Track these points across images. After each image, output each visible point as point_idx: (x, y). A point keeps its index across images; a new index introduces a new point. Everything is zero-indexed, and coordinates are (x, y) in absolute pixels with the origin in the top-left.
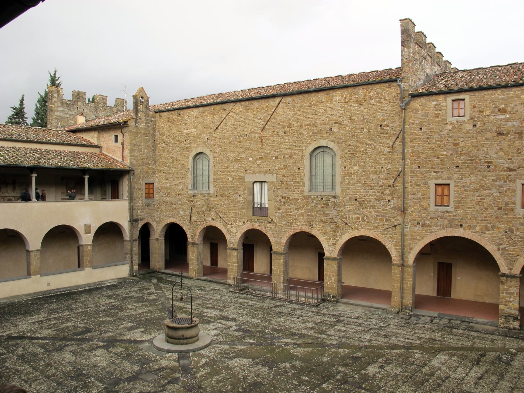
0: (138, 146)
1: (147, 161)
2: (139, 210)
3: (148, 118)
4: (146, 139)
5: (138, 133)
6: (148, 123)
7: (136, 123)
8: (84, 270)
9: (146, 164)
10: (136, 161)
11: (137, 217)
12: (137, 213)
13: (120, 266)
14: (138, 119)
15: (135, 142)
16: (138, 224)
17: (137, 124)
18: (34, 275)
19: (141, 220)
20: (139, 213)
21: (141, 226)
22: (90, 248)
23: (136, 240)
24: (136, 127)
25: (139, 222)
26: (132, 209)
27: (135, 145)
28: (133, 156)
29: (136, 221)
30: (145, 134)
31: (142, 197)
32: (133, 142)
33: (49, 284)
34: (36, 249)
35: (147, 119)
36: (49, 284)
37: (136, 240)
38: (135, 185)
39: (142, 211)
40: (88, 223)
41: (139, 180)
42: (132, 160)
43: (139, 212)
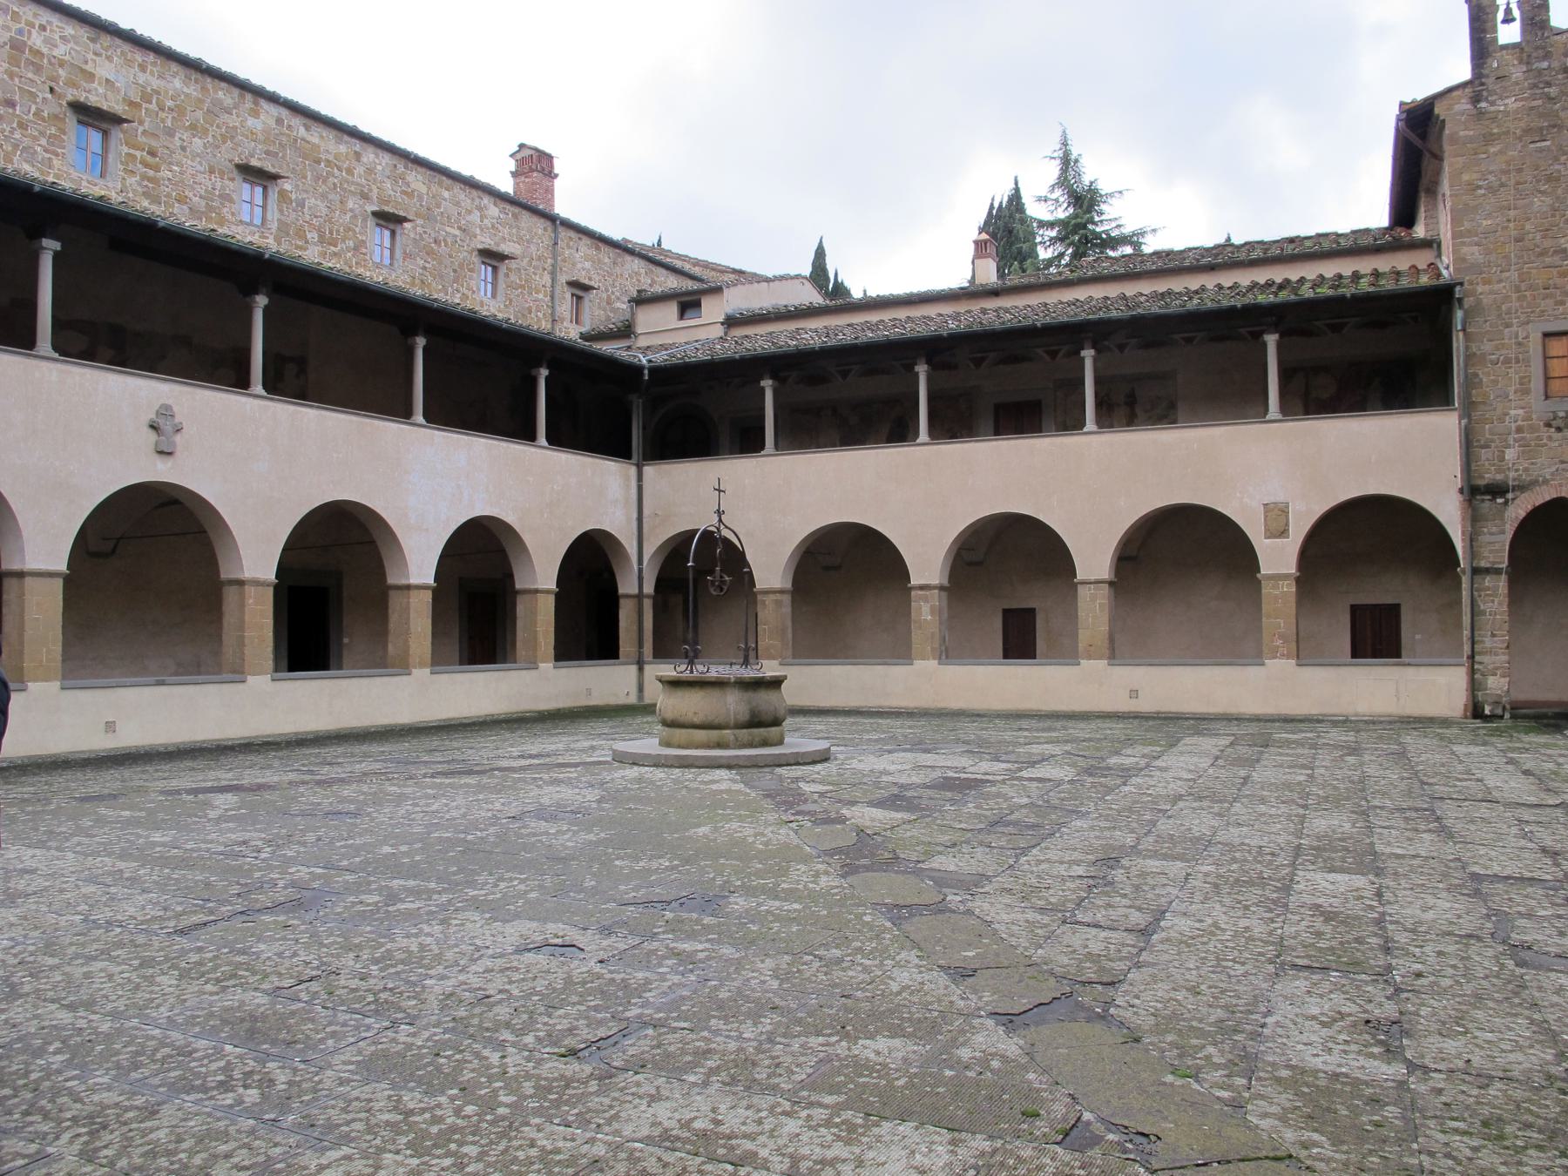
0: (1492, 190)
1: (1547, 243)
2: (1508, 446)
3: (1545, 64)
4: (1541, 150)
5: (1489, 139)
6: (1549, 84)
7: (1476, 99)
8: (1263, 664)
9: (1543, 253)
10: (1488, 253)
11: (1499, 477)
12: (1502, 459)
13: (1422, 669)
14: (1490, 81)
15: (1475, 176)
16: (1506, 503)
17: (1483, 104)
18: (1090, 658)
19: (1522, 488)
20: (1509, 462)
21: (1522, 514)
22: (1289, 588)
23: (1498, 572)
24: (1481, 114)
25: (1510, 496)
26: (1469, 444)
27: (1480, 187)
28: (1469, 233)
29: (1497, 490)
30: (1527, 131)
31: (1527, 392)
32: (1466, 177)
33: (1134, 694)
34: (1093, 578)
35: (1540, 72)
36: (1134, 694)
37: (1498, 572)
38: (1487, 347)
39: (1528, 451)
40: (1280, 497)
41: (1508, 326)
42: (1465, 249)
43: (1510, 454)
